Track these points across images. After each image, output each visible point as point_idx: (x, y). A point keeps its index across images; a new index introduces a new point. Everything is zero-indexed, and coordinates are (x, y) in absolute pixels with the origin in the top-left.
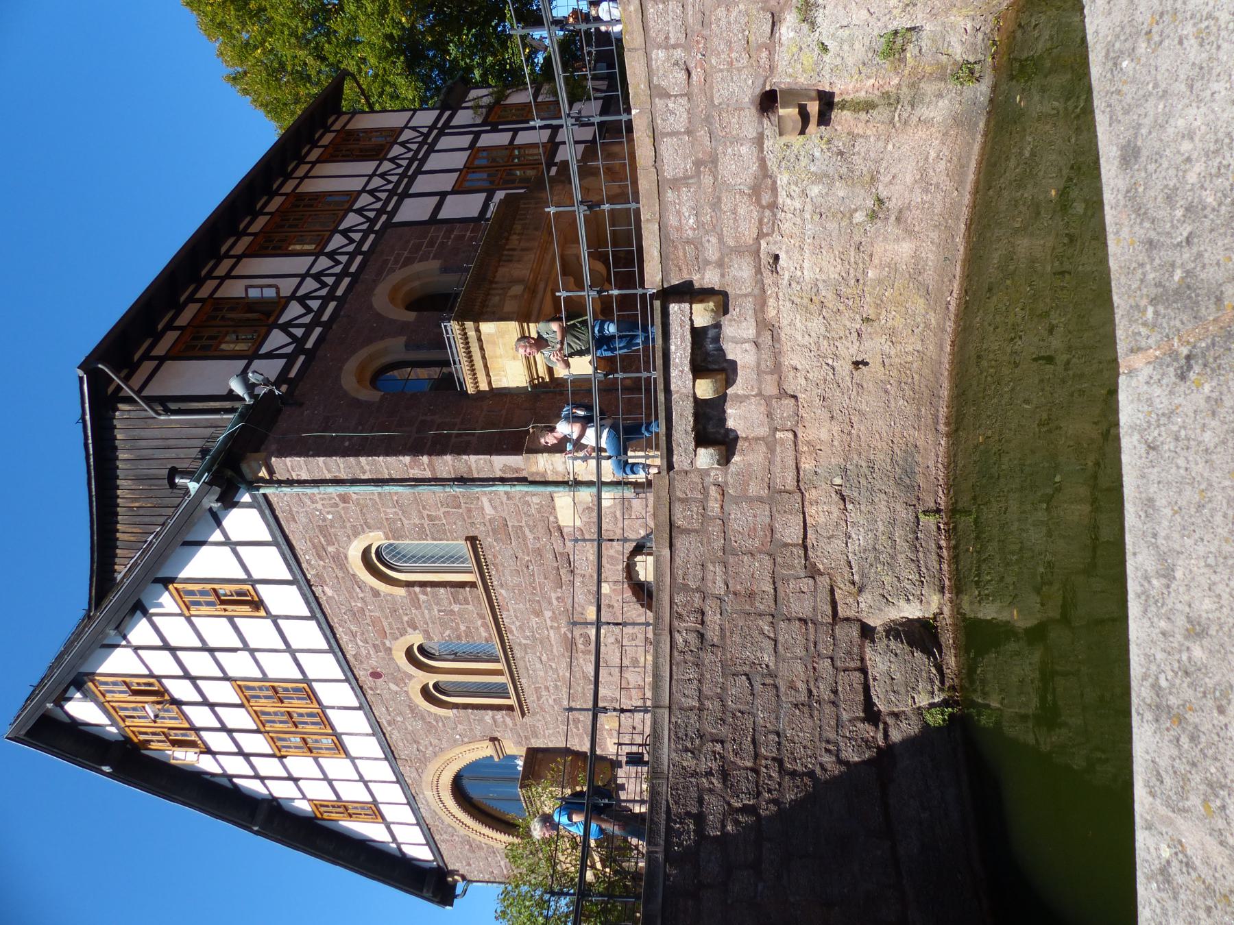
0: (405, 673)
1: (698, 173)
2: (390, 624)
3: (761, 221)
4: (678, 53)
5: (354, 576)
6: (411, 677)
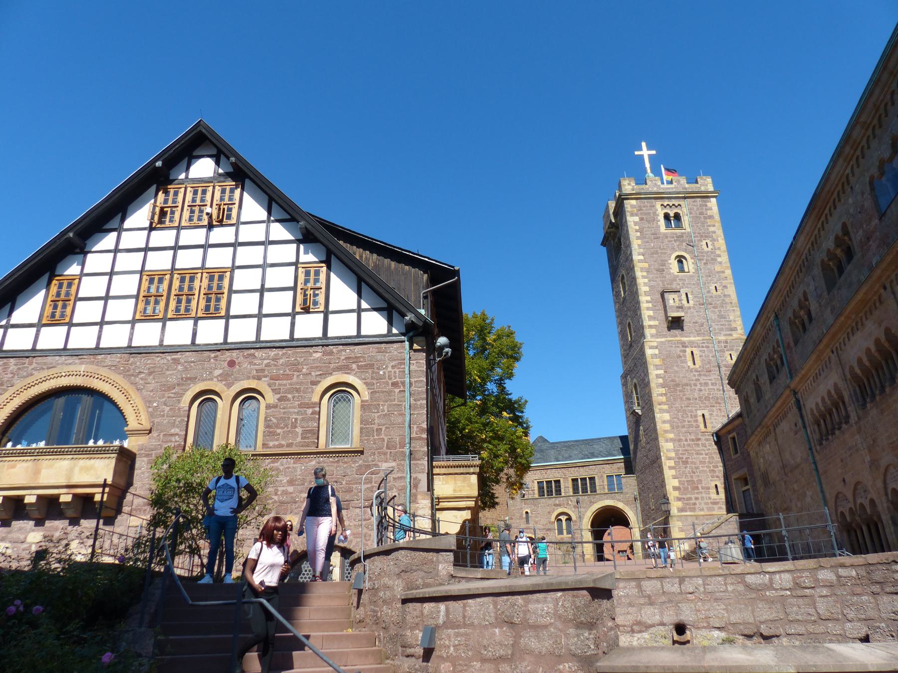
0: (233, 384)
1: (645, 597)
2: (285, 385)
3: (624, 626)
4: (702, 589)
5: (331, 374)
6: (229, 386)
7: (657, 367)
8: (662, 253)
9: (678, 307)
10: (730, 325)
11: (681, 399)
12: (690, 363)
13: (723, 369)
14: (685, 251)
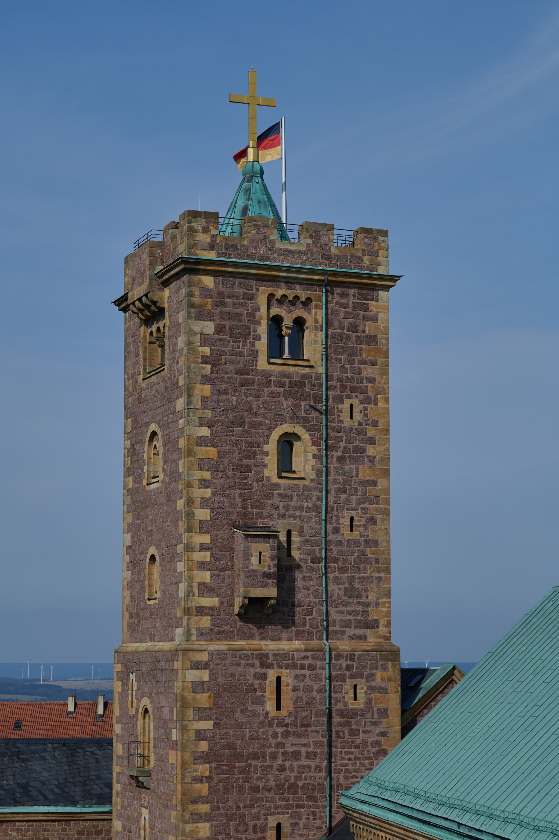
7: (201, 714)
8: (252, 425)
9: (267, 575)
10: (365, 613)
11: (240, 789)
12: (270, 706)
13: (336, 719)
14: (303, 422)
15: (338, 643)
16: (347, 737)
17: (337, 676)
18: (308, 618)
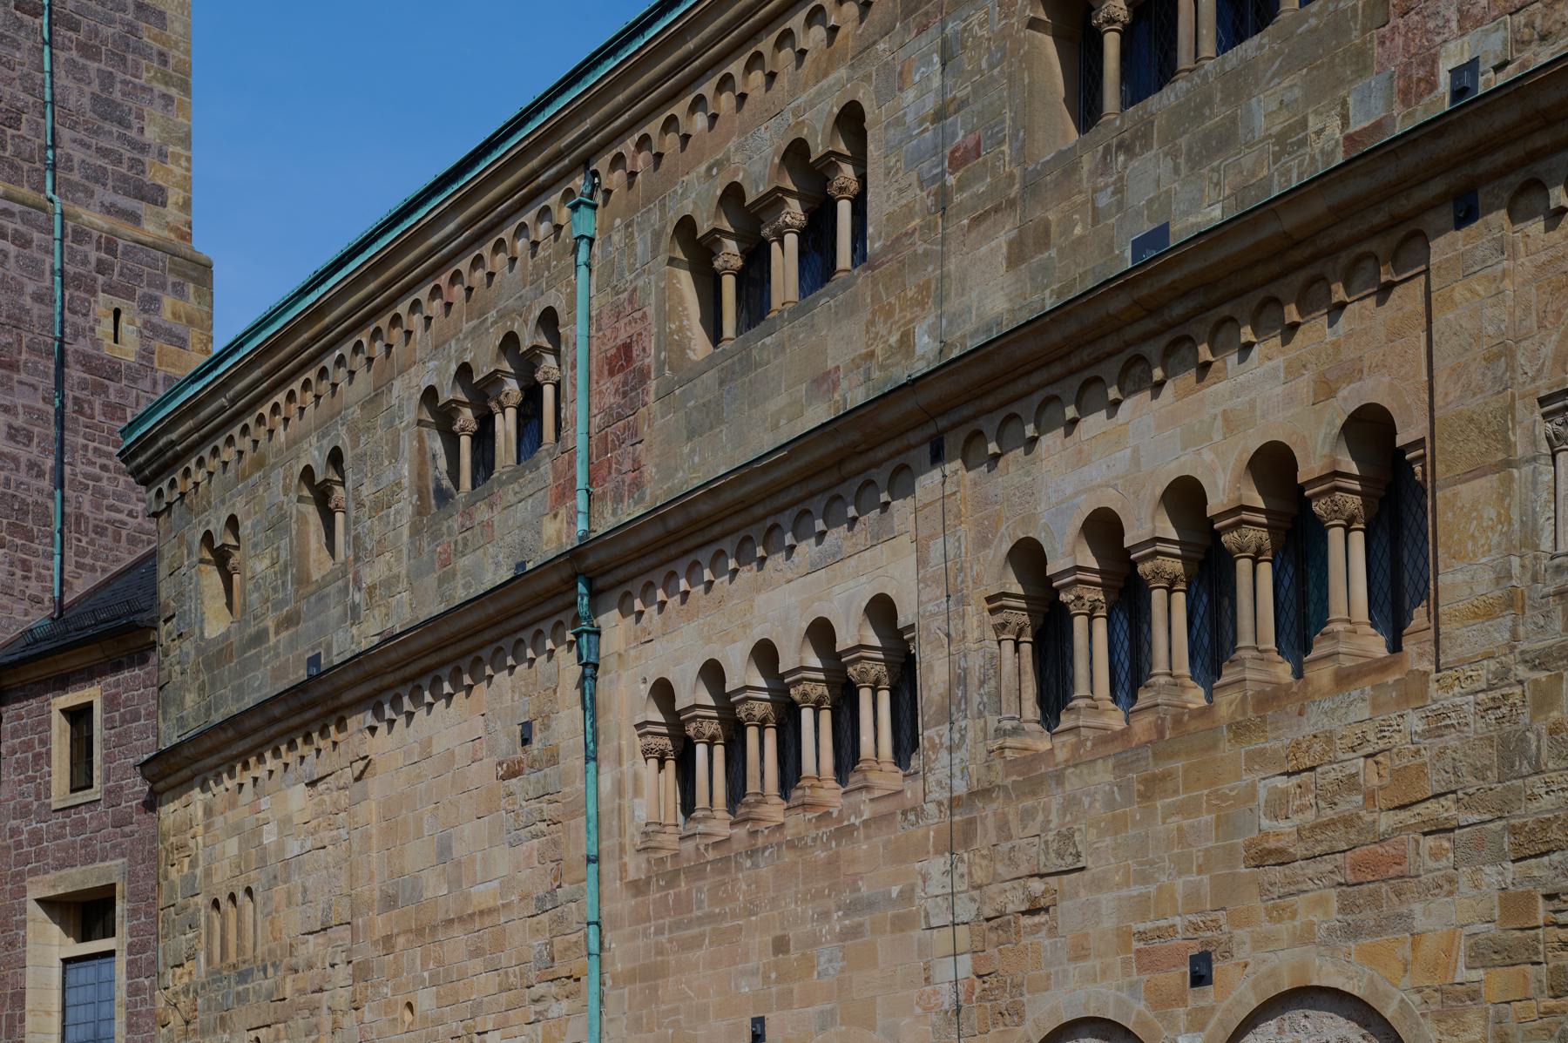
15: (79, 210)
16: (99, 417)
17: (77, 277)
18: (10, 132)
